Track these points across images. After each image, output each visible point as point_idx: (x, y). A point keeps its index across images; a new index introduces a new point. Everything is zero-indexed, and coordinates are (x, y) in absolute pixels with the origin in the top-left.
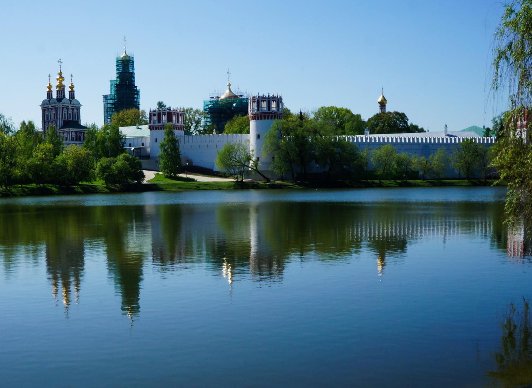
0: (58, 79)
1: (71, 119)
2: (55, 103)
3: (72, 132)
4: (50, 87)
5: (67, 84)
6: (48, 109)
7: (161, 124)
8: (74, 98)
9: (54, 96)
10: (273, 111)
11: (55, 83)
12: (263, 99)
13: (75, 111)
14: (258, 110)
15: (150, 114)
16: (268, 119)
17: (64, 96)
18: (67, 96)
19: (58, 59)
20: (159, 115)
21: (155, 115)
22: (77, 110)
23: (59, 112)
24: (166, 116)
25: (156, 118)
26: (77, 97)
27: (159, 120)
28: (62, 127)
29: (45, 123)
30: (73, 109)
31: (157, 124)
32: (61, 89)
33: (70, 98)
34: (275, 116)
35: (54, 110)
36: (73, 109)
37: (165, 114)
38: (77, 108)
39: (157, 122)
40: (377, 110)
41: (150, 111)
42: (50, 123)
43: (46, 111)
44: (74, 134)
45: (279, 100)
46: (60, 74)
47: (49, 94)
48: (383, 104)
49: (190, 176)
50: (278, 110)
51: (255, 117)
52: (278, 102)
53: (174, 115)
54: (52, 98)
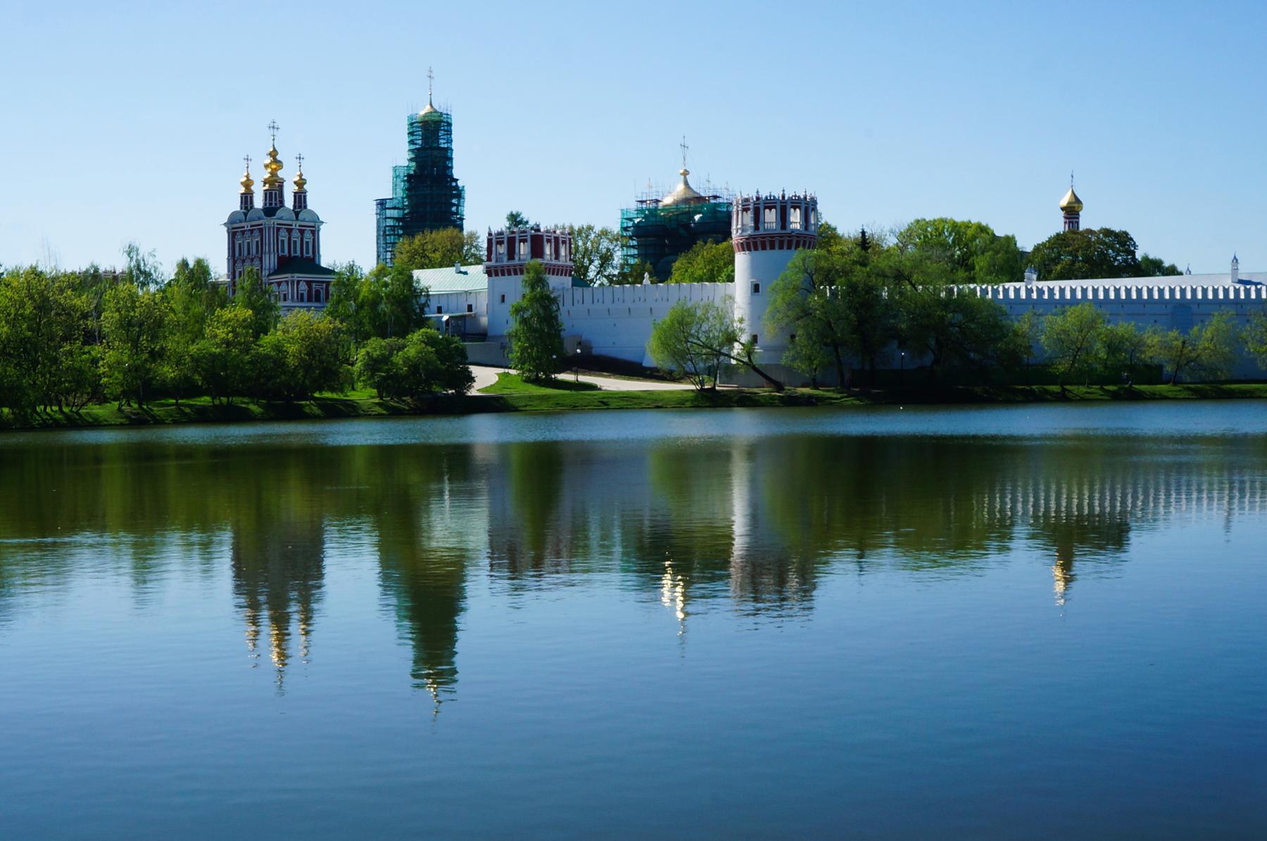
0: (266, 166)
1: (298, 253)
2: (260, 219)
3: (298, 282)
4: (248, 184)
5: (289, 176)
6: (243, 232)
7: (516, 262)
8: (305, 207)
9: (259, 202)
10: (793, 231)
11: (260, 176)
12: (770, 203)
13: (308, 235)
14: (756, 228)
15: (490, 241)
16: (781, 248)
17: (282, 202)
18: (289, 202)
19: (269, 122)
20: (511, 243)
21: (500, 243)
22: (313, 232)
23: (269, 237)
24: (528, 244)
25: (502, 249)
26: (312, 204)
27: (511, 253)
28: (276, 272)
29: (235, 262)
30: (302, 232)
31: (505, 262)
32: (274, 189)
35: (256, 233)
36: (302, 232)
37: (525, 241)
38: (313, 228)
39: (505, 258)
41: (490, 234)
42: (247, 264)
43: (239, 236)
44: (303, 287)
46: (273, 154)
47: (247, 199)
50: (806, 228)
51: (748, 245)
53: (549, 241)
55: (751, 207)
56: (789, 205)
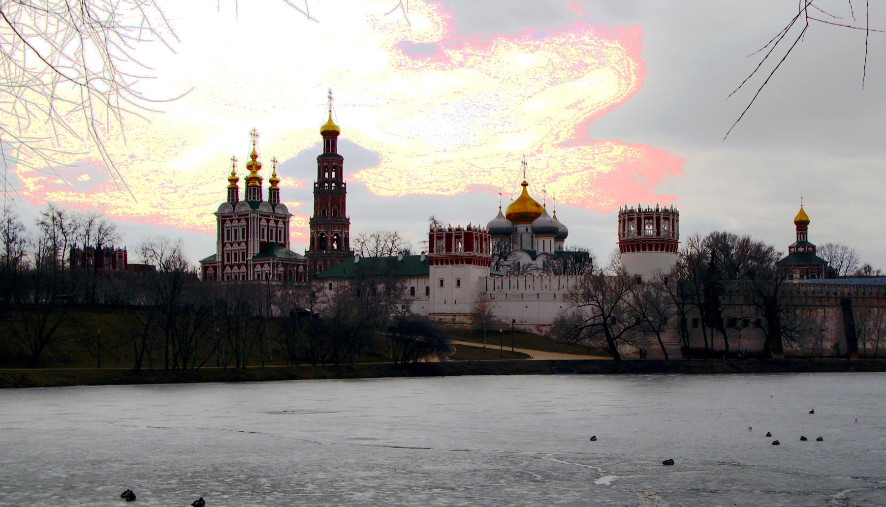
1: (274, 241)
4: (234, 180)
5: (265, 174)
6: (232, 221)
9: (242, 197)
11: (243, 173)
12: (648, 215)
13: (281, 225)
14: (639, 233)
15: (431, 237)
18: (266, 198)
22: (284, 223)
23: (254, 227)
24: (462, 240)
29: (224, 245)
30: (277, 222)
32: (253, 184)
34: (668, 245)
36: (277, 222)
40: (792, 238)
41: (431, 231)
43: (228, 224)
45: (671, 216)
46: (254, 156)
47: (233, 191)
48: (802, 225)
49: (515, 350)
52: (673, 220)
54: (237, 199)
55: (635, 217)
56: (662, 217)
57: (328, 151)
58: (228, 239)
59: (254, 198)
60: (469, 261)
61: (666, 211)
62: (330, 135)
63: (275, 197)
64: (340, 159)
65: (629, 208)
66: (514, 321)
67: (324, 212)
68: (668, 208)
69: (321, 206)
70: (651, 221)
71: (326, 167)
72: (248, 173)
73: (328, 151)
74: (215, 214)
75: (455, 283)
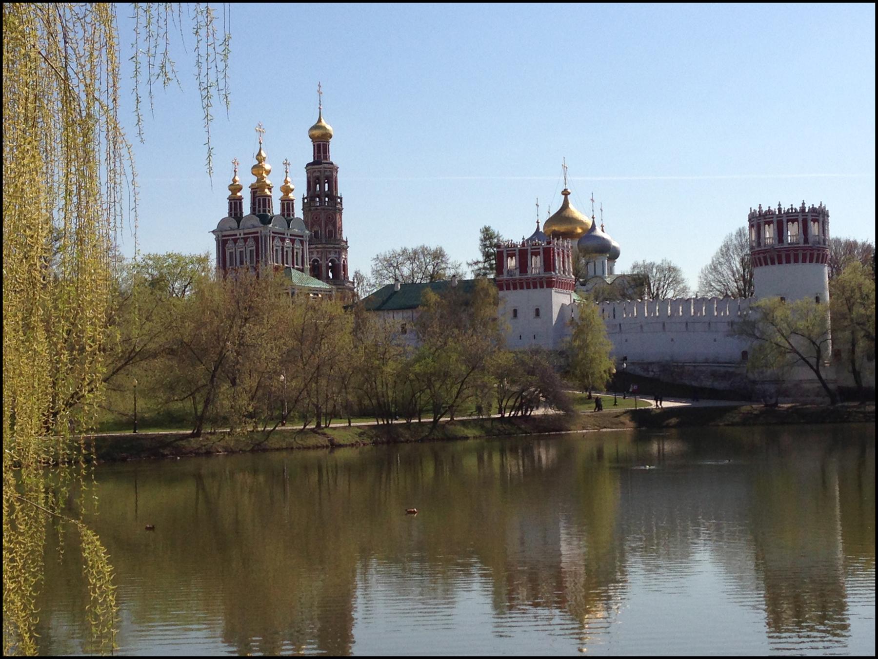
2: (254, 227)
4: (235, 188)
6: (235, 241)
9: (246, 210)
11: (247, 180)
12: (792, 216)
18: (276, 209)
21: (511, 256)
25: (512, 263)
27: (523, 266)
33: (283, 215)
34: (818, 255)
36: (293, 241)
37: (536, 254)
43: (230, 244)
47: (235, 204)
54: (241, 213)
55: (775, 219)
56: (810, 218)
57: (319, 157)
58: (231, 264)
59: (264, 211)
60: (550, 284)
61: (813, 210)
62: (321, 142)
63: (288, 210)
64: (333, 169)
65: (765, 209)
66: (625, 359)
67: (316, 233)
68: (817, 206)
69: (312, 225)
70: (796, 223)
71: (318, 178)
72: (254, 179)
73: (319, 157)
74: (213, 232)
75: (533, 313)
